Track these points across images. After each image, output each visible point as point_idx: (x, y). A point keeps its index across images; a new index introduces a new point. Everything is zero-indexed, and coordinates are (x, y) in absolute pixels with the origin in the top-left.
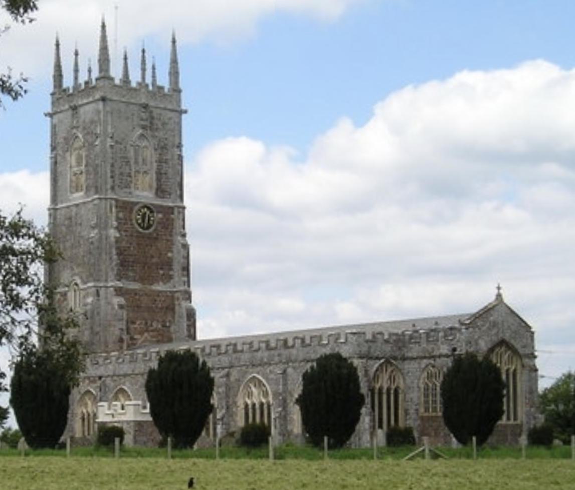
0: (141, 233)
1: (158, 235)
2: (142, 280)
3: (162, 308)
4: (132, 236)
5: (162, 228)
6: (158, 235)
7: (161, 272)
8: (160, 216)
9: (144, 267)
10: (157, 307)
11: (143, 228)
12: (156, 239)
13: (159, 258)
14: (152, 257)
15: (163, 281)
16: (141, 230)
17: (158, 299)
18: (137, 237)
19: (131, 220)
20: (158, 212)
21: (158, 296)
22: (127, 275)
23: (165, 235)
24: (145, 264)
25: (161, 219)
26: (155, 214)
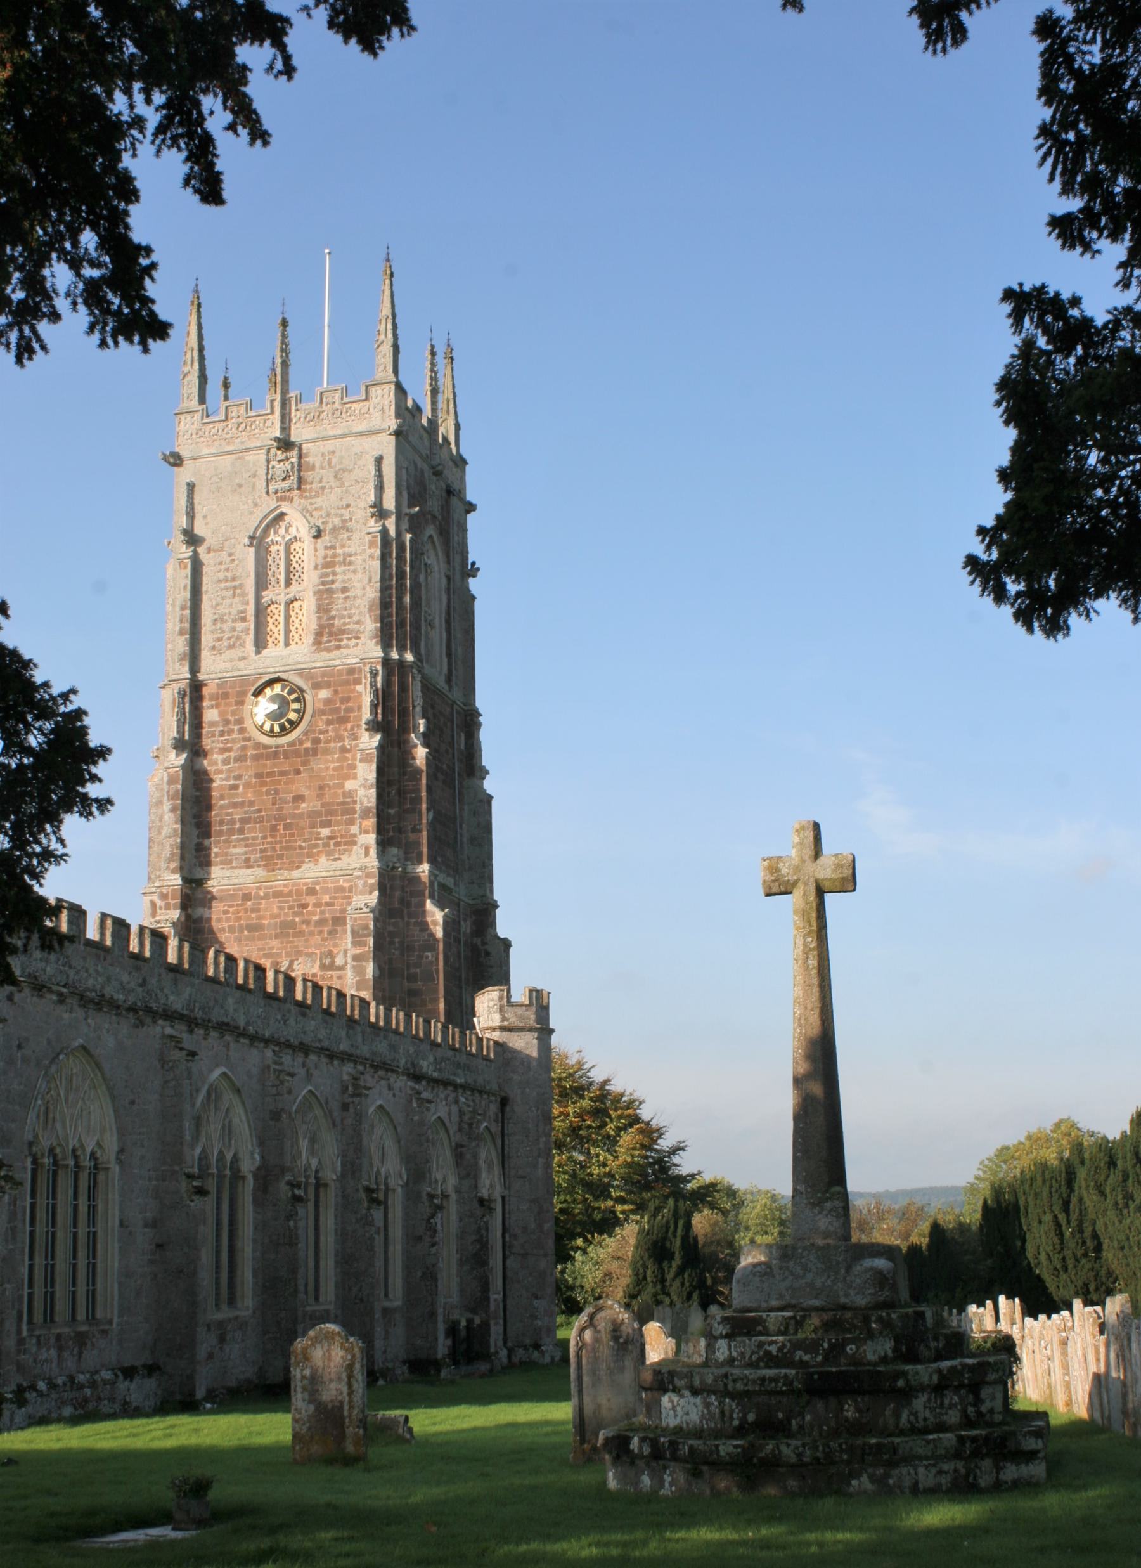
0: (266, 747)
1: (316, 741)
2: (269, 861)
3: (322, 922)
4: (240, 759)
5: (329, 723)
6: (316, 741)
7: (325, 832)
8: (324, 694)
9: (274, 828)
10: (308, 922)
11: (271, 733)
12: (315, 752)
13: (320, 796)
14: (299, 798)
15: (329, 853)
16: (265, 740)
17: (311, 900)
18: (256, 758)
19: (240, 721)
20: (317, 686)
21: (312, 892)
22: (227, 854)
23: (340, 738)
24: (280, 818)
25: (327, 702)
26: (308, 697)
